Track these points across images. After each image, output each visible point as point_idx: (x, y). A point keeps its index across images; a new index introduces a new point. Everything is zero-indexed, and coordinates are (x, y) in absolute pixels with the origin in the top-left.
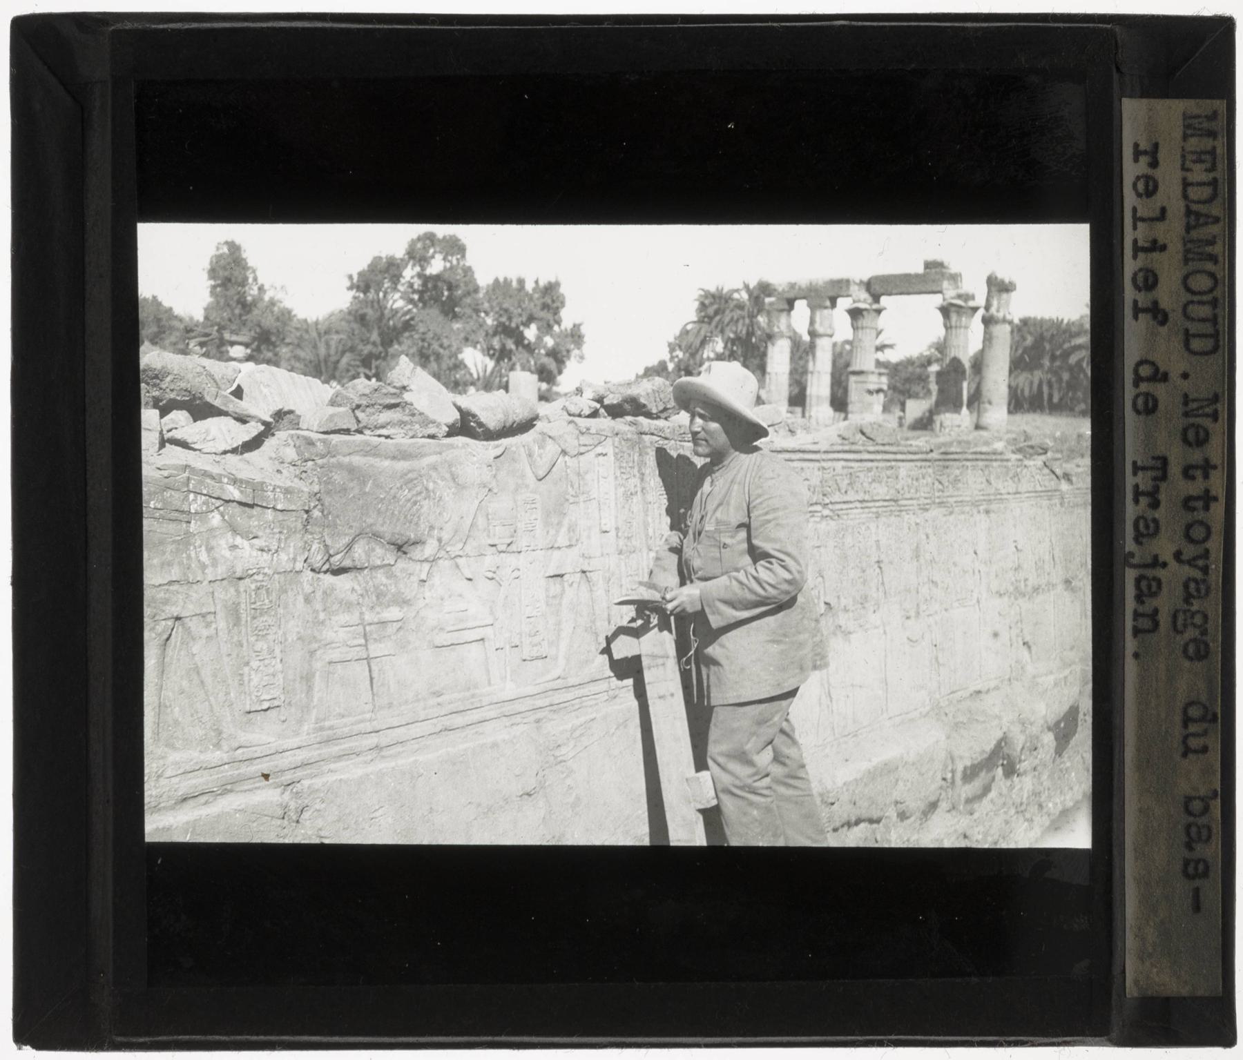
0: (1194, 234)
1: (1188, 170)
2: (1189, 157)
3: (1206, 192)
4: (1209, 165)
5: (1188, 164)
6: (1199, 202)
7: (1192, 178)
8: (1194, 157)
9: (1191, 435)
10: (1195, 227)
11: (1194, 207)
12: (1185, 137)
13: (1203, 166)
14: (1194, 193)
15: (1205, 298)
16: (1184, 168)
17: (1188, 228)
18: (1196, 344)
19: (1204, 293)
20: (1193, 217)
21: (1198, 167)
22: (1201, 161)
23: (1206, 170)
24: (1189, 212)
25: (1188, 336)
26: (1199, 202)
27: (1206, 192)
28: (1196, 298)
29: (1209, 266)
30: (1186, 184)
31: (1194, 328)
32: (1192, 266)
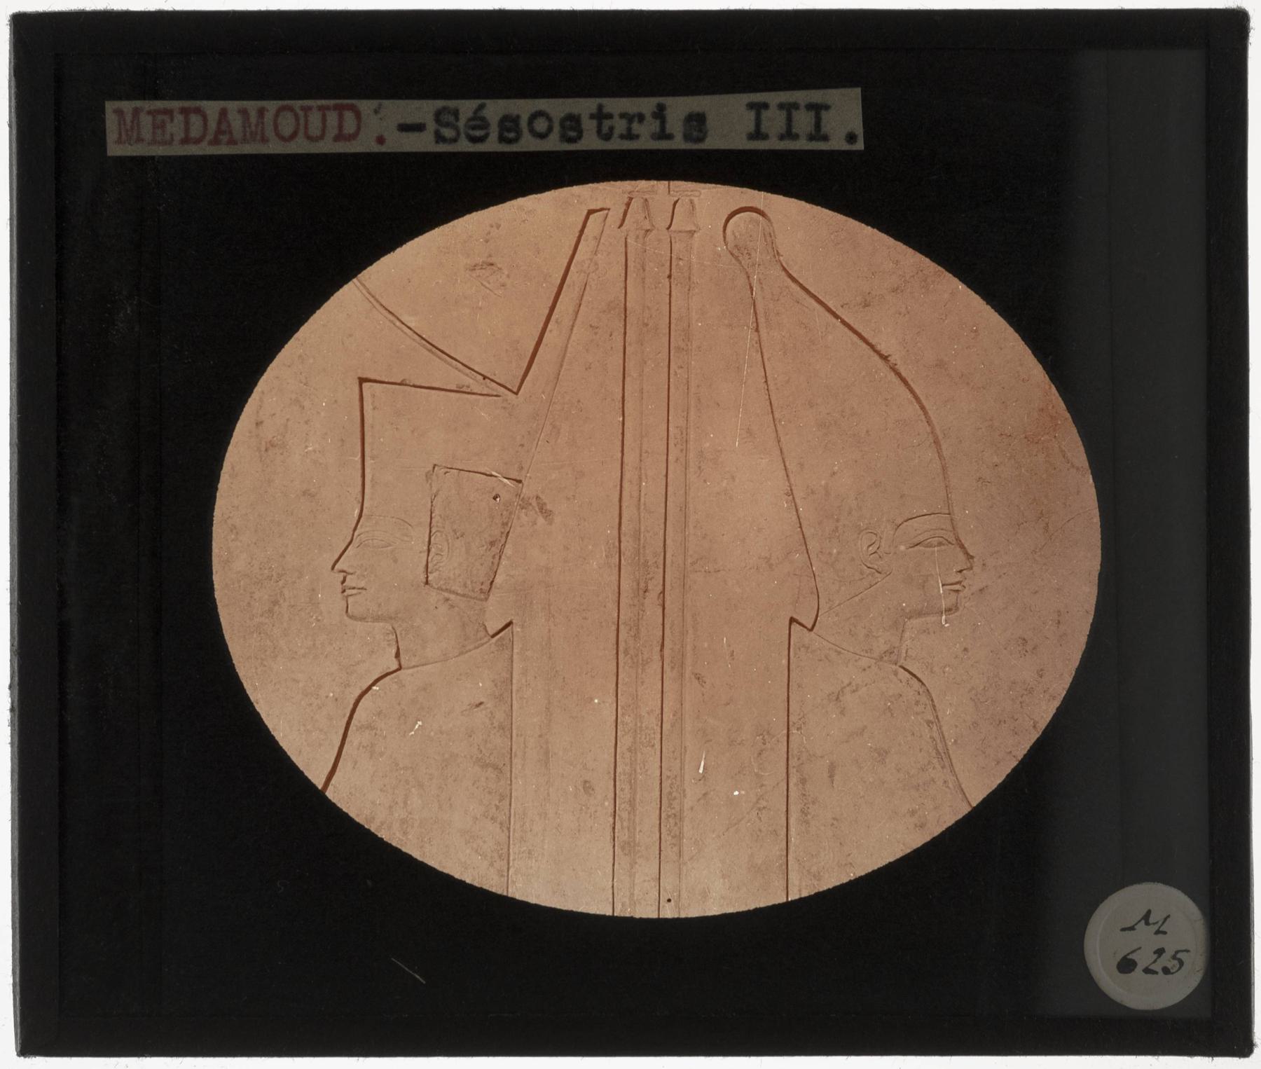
0: (238, 134)
3: (195, 120)
4: (166, 118)
5: (168, 137)
7: (180, 135)
8: (159, 131)
12: (140, 140)
14: (195, 132)
15: (302, 121)
19: (297, 119)
21: (169, 126)
22: (163, 126)
23: (172, 120)
25: (339, 137)
27: (195, 120)
28: (302, 127)
29: (269, 116)
30: (186, 140)
31: (332, 132)
32: (270, 132)
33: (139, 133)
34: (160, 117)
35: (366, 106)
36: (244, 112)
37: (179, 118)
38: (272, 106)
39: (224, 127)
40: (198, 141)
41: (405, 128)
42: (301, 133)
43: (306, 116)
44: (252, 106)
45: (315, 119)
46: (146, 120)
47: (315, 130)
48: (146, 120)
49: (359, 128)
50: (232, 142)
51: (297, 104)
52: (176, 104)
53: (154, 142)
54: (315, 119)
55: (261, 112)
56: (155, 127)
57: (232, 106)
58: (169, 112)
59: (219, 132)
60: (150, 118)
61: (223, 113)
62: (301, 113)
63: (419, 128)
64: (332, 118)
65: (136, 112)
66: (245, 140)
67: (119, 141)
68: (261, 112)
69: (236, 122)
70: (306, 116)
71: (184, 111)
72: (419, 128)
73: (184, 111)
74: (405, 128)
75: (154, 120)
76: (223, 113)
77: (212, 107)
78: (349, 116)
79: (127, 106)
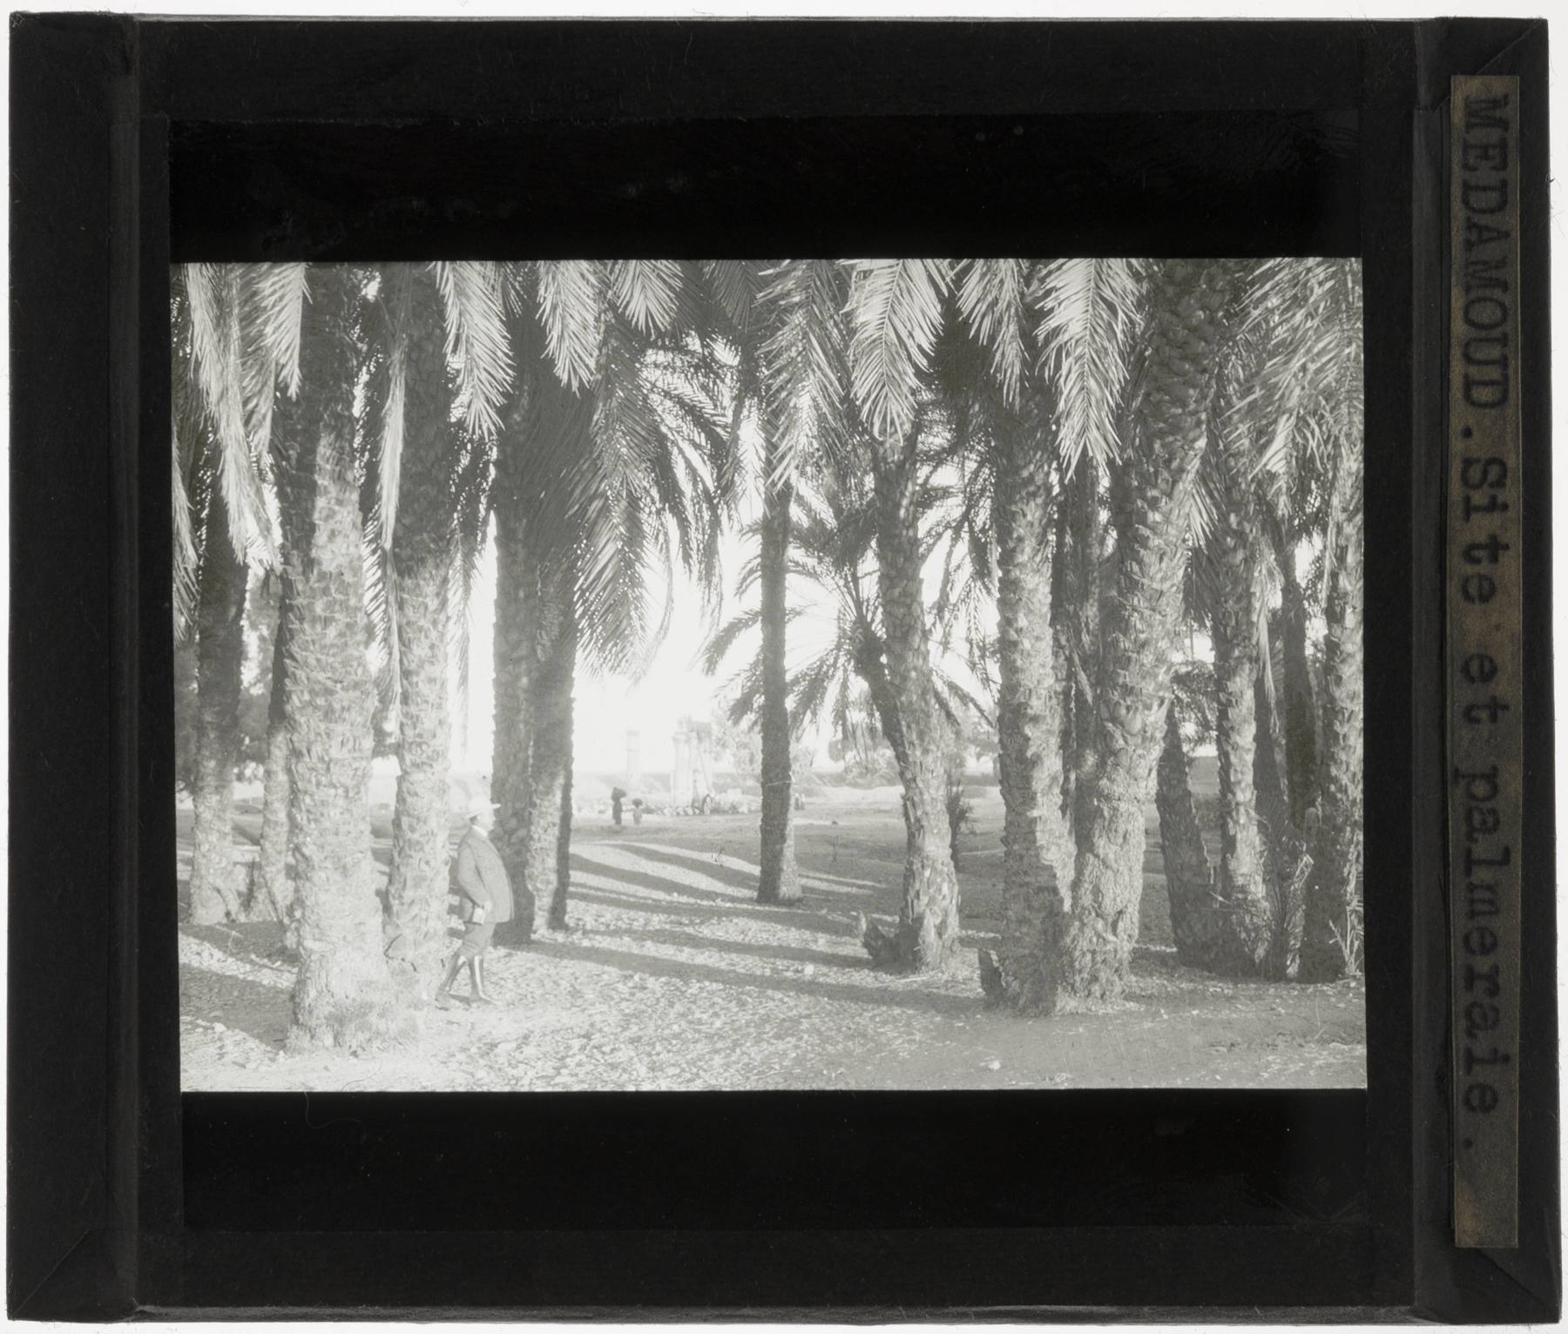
1: (1475, 169)
6: (1483, 212)
11: (1476, 218)
17: (1469, 245)
22: (1486, 157)
23: (1495, 168)
24: (1470, 226)
25: (1468, 384)
26: (1483, 212)
27: (1493, 198)
28: (1483, 334)
29: (1497, 293)
30: (1467, 187)
33: (1476, 125)
37: (1493, 178)
40: (1466, 202)
42: (1474, 333)
43: (1496, 340)
45: (1495, 352)
48: (1494, 135)
54: (1495, 352)
56: (1486, 148)
58: (1504, 166)
59: (1481, 229)
64: (1494, 373)
65: (1504, 124)
69: (1491, 251)
71: (1504, 184)
75: (1494, 147)
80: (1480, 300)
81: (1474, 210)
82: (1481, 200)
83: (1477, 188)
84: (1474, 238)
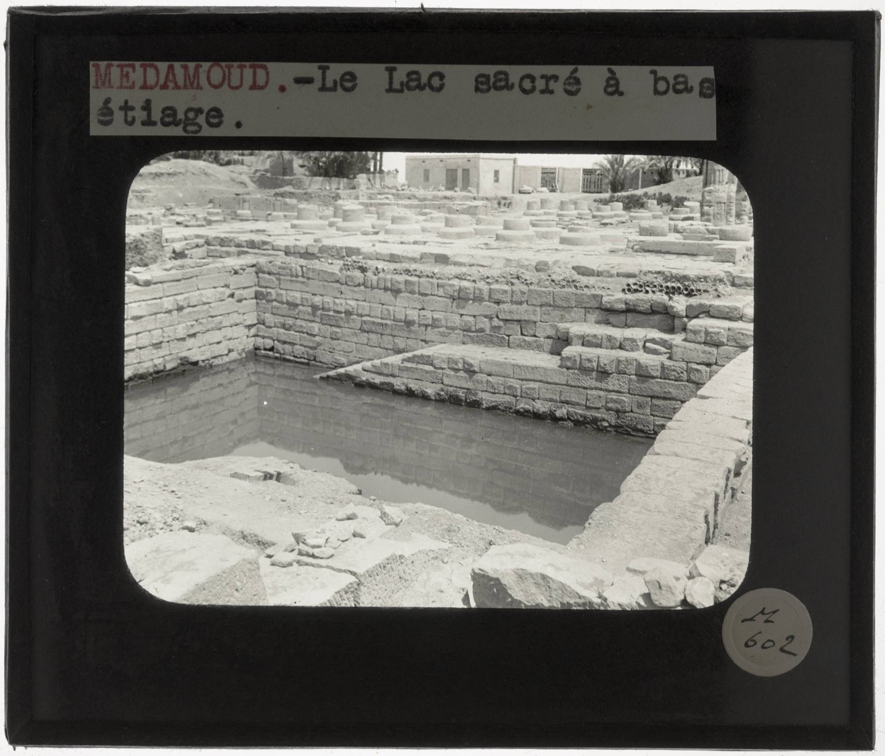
0: (180, 81)
1: (134, 83)
2: (125, 84)
3: (151, 72)
4: (130, 70)
5: (130, 84)
6: (158, 77)
7: (139, 83)
8: (125, 80)
9: (348, 85)
10: (176, 84)
11: (162, 82)
13: (131, 75)
16: (132, 87)
18: (261, 81)
20: (169, 84)
23: (134, 72)
24: (164, 87)
25: (254, 87)
26: (158, 77)
27: (151, 72)
30: (144, 87)
34: (126, 69)
35: (271, 65)
36: (186, 68)
37: (139, 70)
38: (206, 65)
39: (171, 77)
40: (152, 88)
41: (298, 81)
42: (226, 82)
43: (229, 72)
44: (192, 65)
46: (115, 72)
47: (235, 82)
48: (115, 72)
49: (267, 83)
50: (177, 87)
51: (223, 64)
52: (137, 64)
53: (121, 87)
54: (235, 72)
55: (197, 67)
57: (177, 65)
60: (119, 69)
61: (171, 68)
62: (227, 70)
63: (309, 81)
64: (248, 72)
66: (185, 87)
67: (97, 87)
68: (197, 67)
70: (229, 72)
72: (309, 81)
73: (144, 67)
74: (298, 81)
75: (122, 71)
76: (171, 68)
77: (163, 66)
78: (261, 73)
79: (103, 64)
80: (208, 78)
81: (157, 83)
82: (151, 80)
83: (145, 81)
84: (171, 85)
